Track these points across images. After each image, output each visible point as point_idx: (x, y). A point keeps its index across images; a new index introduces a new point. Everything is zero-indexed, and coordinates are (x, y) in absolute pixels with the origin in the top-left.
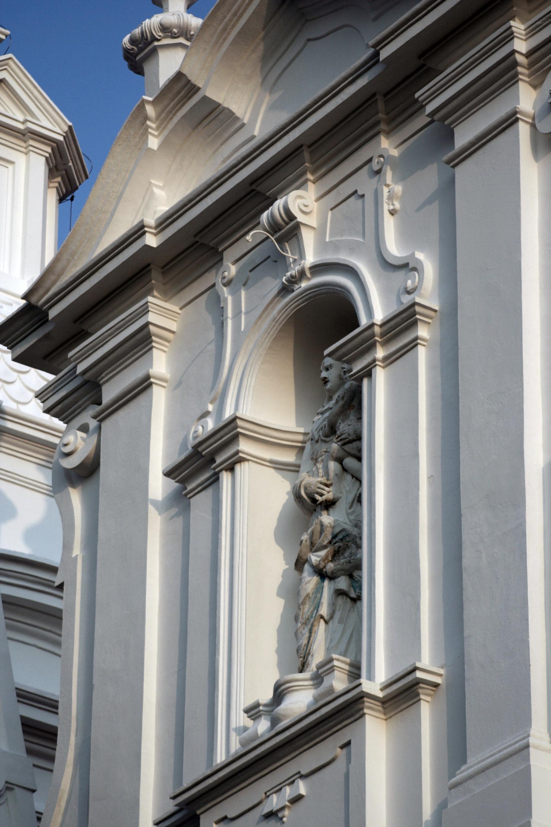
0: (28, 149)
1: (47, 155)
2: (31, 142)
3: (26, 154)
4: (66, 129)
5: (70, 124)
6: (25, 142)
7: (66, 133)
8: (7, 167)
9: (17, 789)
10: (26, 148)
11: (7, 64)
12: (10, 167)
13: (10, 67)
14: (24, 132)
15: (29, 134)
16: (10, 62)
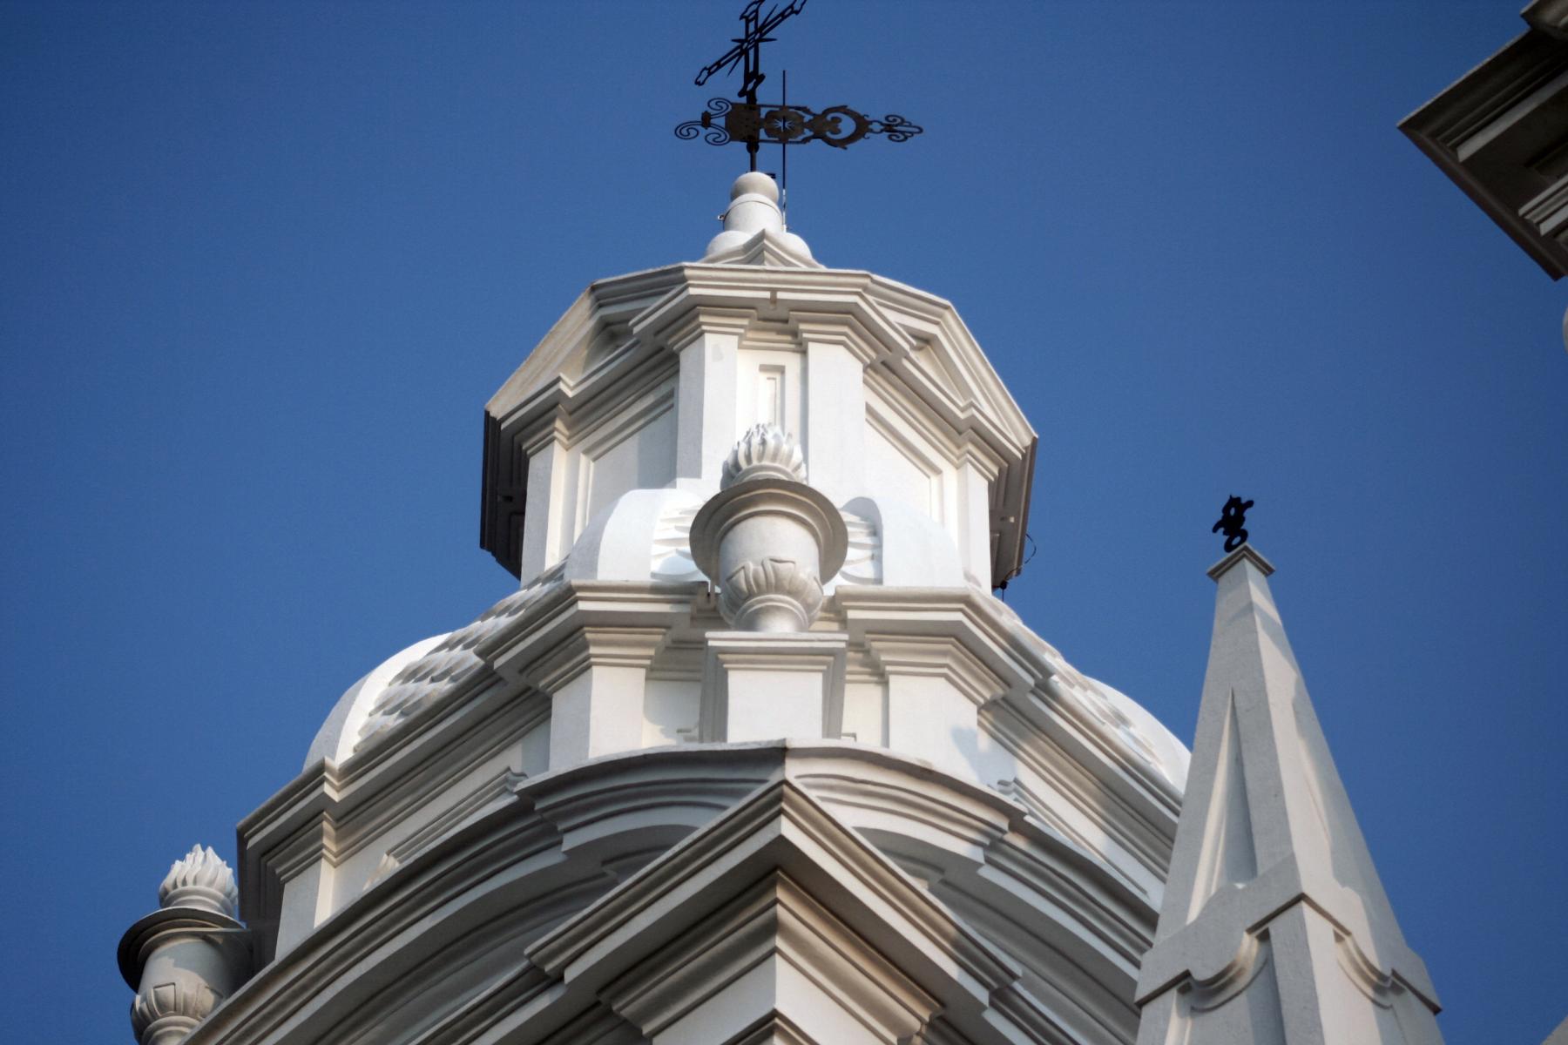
0: (963, 459)
1: (992, 479)
2: (971, 447)
3: (957, 468)
4: (1028, 442)
5: (1037, 436)
6: (959, 447)
7: (1026, 448)
8: (929, 477)
9: (1409, 994)
10: (958, 458)
11: (940, 316)
12: (934, 479)
13: (945, 322)
14: (961, 428)
15: (970, 430)
16: (947, 314)
